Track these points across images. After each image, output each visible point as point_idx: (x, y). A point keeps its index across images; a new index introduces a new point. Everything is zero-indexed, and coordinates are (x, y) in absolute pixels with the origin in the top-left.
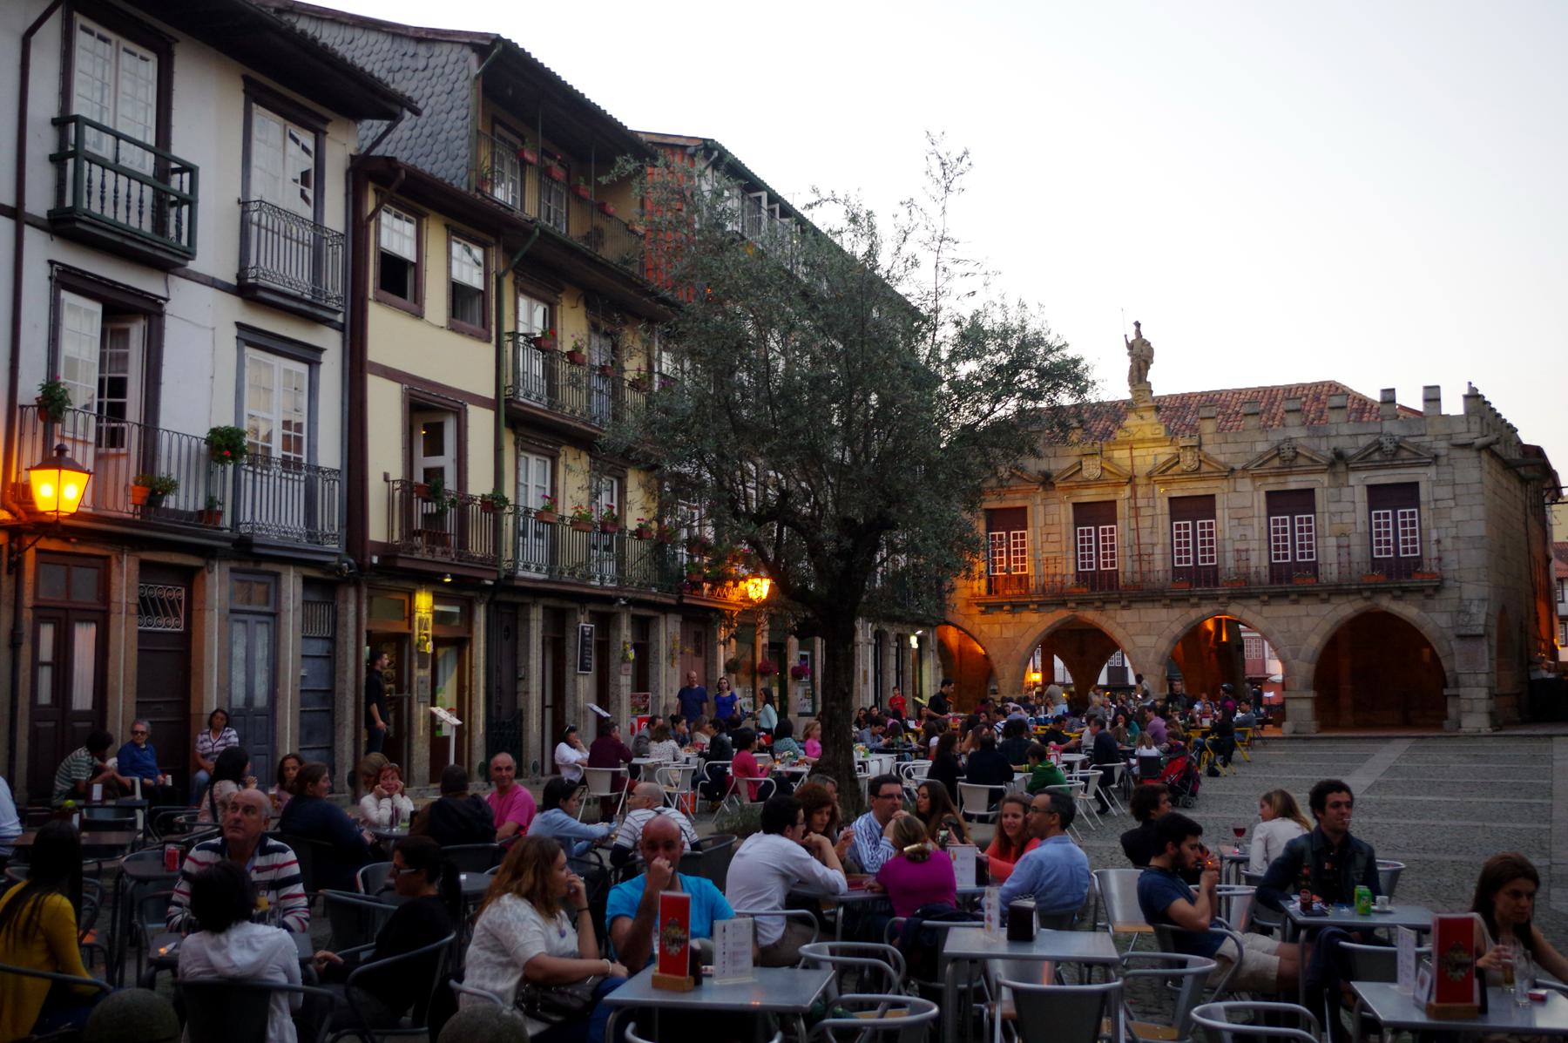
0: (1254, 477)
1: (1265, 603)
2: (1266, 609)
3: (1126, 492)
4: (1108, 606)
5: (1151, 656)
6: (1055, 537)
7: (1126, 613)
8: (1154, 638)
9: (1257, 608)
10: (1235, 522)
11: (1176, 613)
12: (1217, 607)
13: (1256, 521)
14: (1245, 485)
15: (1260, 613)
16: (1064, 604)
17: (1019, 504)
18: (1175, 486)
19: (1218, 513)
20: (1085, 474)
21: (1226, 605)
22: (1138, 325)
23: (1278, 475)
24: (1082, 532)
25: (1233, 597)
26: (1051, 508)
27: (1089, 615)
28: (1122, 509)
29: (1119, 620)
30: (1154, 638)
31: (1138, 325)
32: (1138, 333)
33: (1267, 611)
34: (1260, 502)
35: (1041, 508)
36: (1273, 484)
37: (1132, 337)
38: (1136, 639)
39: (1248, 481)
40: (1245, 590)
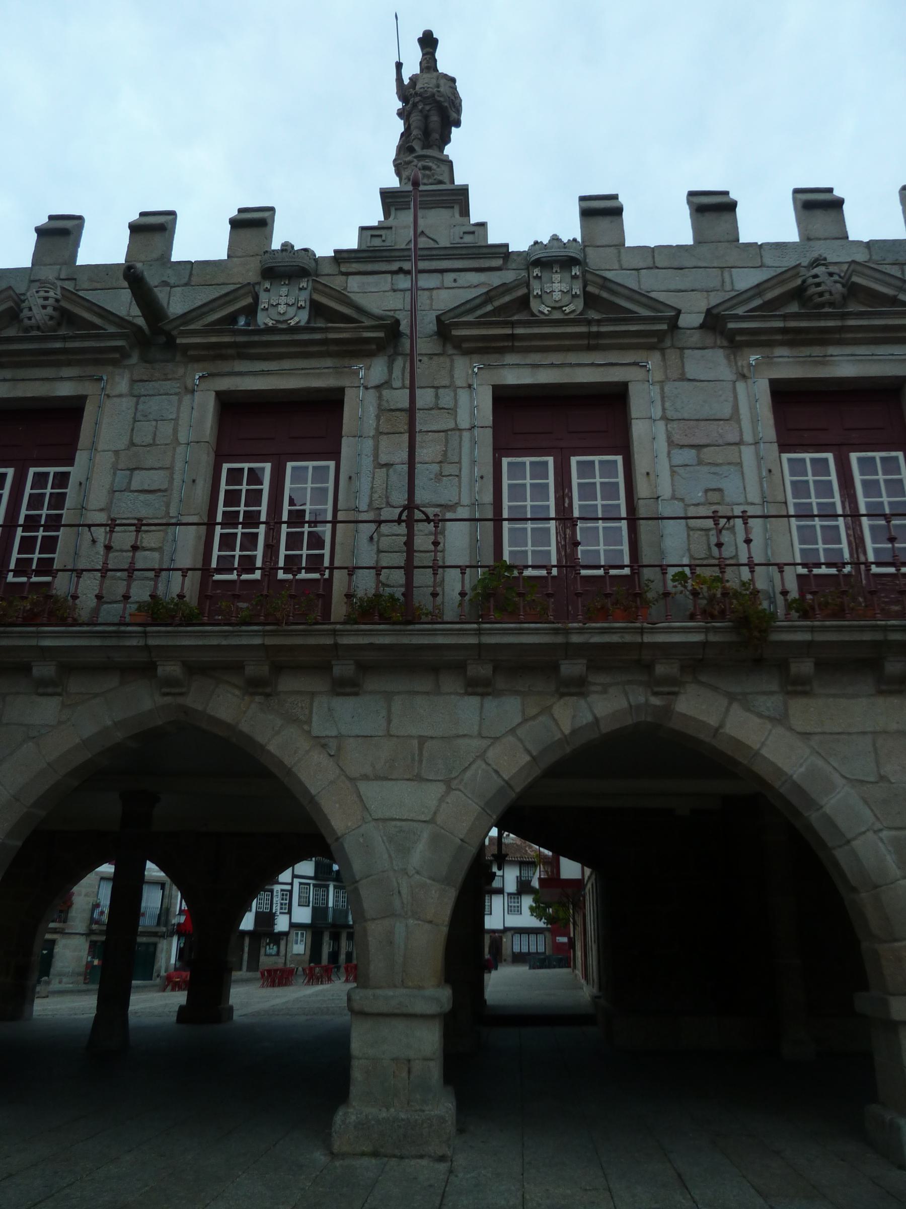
0: (735, 343)
1: (796, 687)
2: (797, 705)
3: (375, 370)
4: (287, 683)
5: (419, 853)
6: (156, 479)
7: (345, 706)
8: (436, 790)
9: (771, 703)
10: (689, 456)
11: (507, 710)
12: (640, 696)
13: (748, 454)
14: (710, 364)
15: (781, 720)
16: (141, 667)
17: (65, 389)
18: (510, 359)
19: (639, 429)
20: (263, 320)
21: (671, 687)
22: (428, 42)
23: (795, 338)
24: (235, 476)
25: (698, 663)
26: (153, 405)
27: (226, 705)
28: (360, 411)
29: (318, 728)
30: (436, 790)
31: (428, 42)
32: (429, 62)
33: (806, 713)
34: (754, 404)
35: (127, 403)
36: (790, 366)
37: (412, 68)
38: (368, 789)
39: (719, 356)
40: (744, 637)
